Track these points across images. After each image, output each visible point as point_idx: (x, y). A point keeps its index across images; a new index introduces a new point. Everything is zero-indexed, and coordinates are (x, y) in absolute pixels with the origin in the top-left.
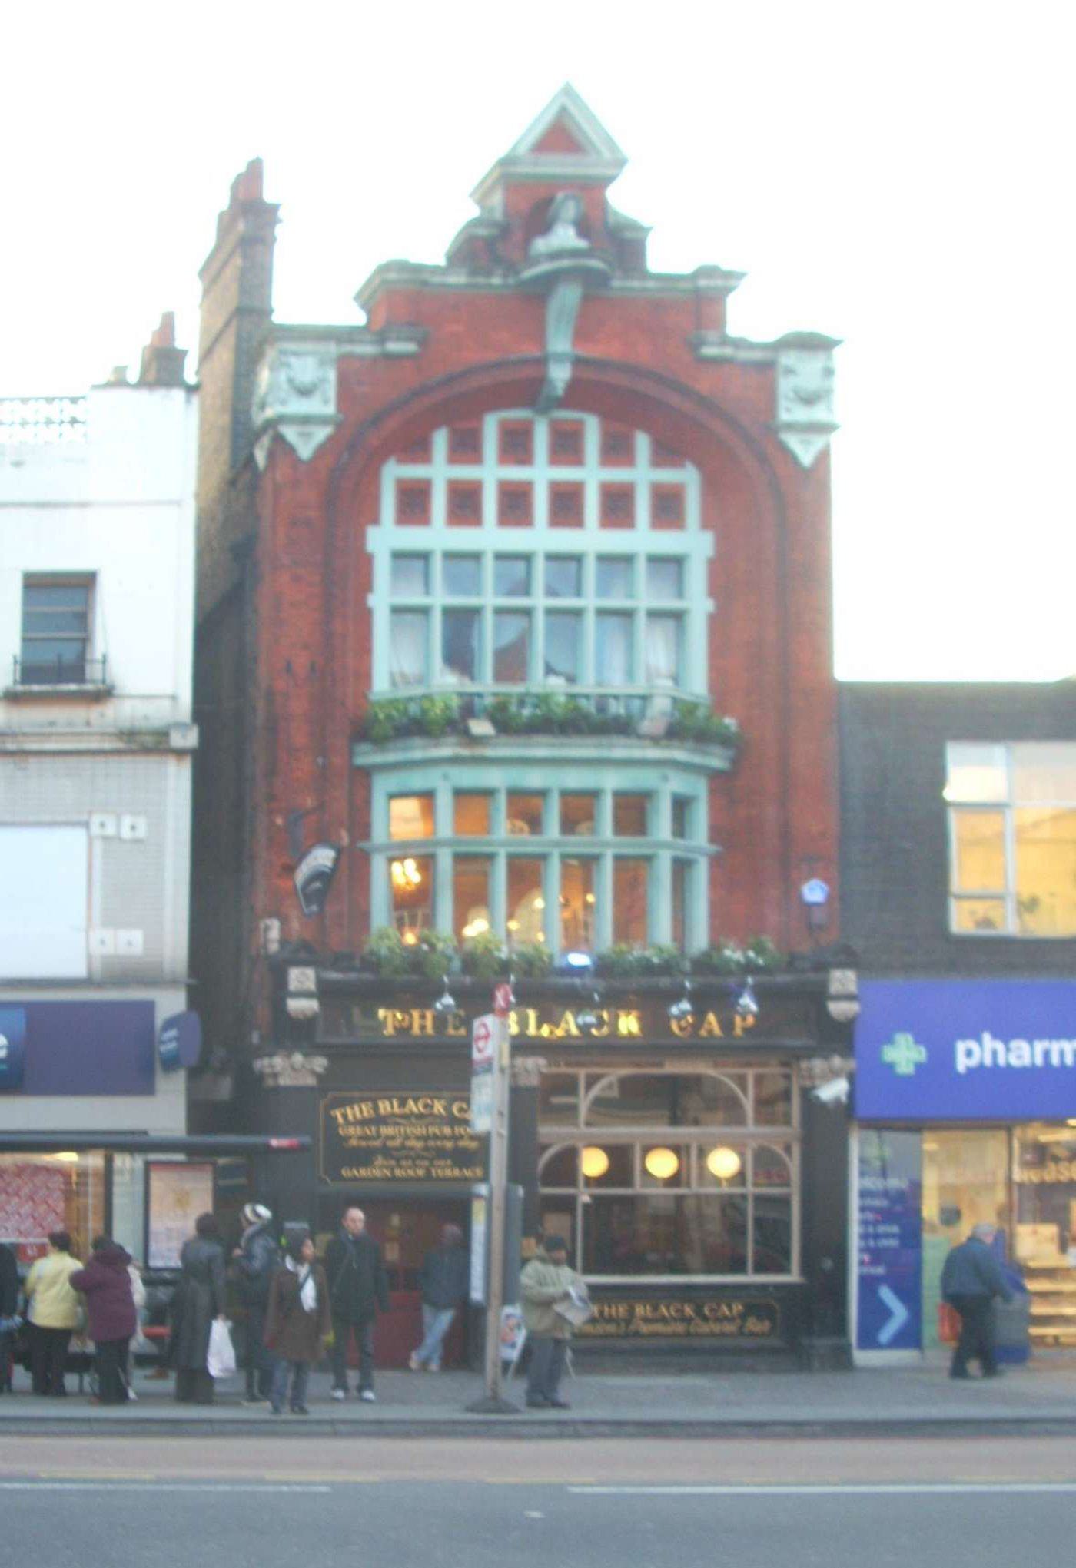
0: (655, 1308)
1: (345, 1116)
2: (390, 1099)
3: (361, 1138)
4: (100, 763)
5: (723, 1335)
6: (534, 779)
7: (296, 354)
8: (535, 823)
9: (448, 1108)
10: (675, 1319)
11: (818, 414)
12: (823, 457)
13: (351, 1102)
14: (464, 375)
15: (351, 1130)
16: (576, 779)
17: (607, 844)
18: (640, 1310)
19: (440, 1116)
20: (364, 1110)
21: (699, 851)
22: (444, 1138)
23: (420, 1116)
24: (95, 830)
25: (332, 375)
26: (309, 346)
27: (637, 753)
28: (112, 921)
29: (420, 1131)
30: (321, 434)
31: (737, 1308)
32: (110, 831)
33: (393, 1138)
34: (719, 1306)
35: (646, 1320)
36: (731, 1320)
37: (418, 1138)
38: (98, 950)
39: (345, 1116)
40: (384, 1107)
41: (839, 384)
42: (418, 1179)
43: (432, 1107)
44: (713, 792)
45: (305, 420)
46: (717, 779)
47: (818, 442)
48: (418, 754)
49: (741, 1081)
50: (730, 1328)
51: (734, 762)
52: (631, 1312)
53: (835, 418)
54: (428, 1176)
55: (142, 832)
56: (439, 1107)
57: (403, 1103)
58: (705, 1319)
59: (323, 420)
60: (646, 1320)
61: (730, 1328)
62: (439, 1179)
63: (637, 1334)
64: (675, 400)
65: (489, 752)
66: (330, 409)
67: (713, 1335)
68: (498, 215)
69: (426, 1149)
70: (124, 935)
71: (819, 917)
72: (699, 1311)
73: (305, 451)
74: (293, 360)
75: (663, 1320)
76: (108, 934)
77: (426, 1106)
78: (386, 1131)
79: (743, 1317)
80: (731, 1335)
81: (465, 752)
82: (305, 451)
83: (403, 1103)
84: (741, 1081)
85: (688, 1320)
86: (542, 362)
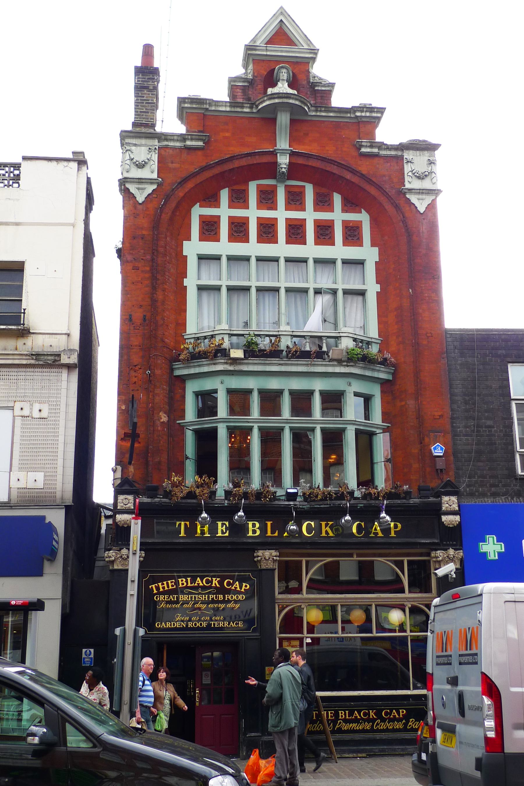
0: (351, 713)
1: (158, 588)
2: (186, 577)
3: (167, 602)
4: (22, 373)
5: (394, 730)
6: (274, 384)
7: (135, 145)
8: (276, 411)
9: (221, 583)
10: (364, 720)
11: (426, 184)
12: (432, 207)
13: (162, 579)
14: (232, 159)
15: (162, 597)
16: (298, 384)
17: (317, 422)
18: (341, 714)
19: (216, 587)
20: (170, 584)
21: (377, 427)
22: (218, 602)
23: (204, 588)
24: (17, 412)
25: (155, 157)
26: (143, 141)
27: (330, 370)
28: (25, 467)
29: (204, 598)
30: (150, 188)
31: (403, 712)
32: (26, 412)
33: (187, 602)
34: (391, 711)
35: (346, 721)
36: (399, 720)
37: (203, 603)
38: (15, 484)
39: (158, 588)
40: (182, 582)
41: (439, 169)
42: (203, 629)
43: (212, 582)
44: (383, 392)
45: (140, 181)
46: (384, 384)
47: (428, 200)
48: (206, 369)
49: (400, 565)
50: (399, 725)
51: (394, 374)
52: (336, 715)
53: (439, 186)
54: (209, 627)
55: (44, 414)
56: (215, 582)
57: (193, 580)
58: (383, 720)
59: (151, 181)
60: (346, 721)
61: (399, 725)
62: (215, 629)
63: (340, 731)
64: (348, 176)
65: (245, 368)
66: (155, 176)
67: (387, 730)
68: (250, 76)
69: (207, 609)
70: (32, 475)
71: (440, 464)
72: (378, 714)
73: (141, 198)
74: (133, 148)
75: (356, 721)
76: (22, 475)
77: (207, 582)
78: (183, 598)
79: (406, 717)
80: (399, 730)
81: (231, 368)
82: (141, 198)
83: (193, 580)
84: (400, 565)
85: (373, 720)
86: (274, 154)
